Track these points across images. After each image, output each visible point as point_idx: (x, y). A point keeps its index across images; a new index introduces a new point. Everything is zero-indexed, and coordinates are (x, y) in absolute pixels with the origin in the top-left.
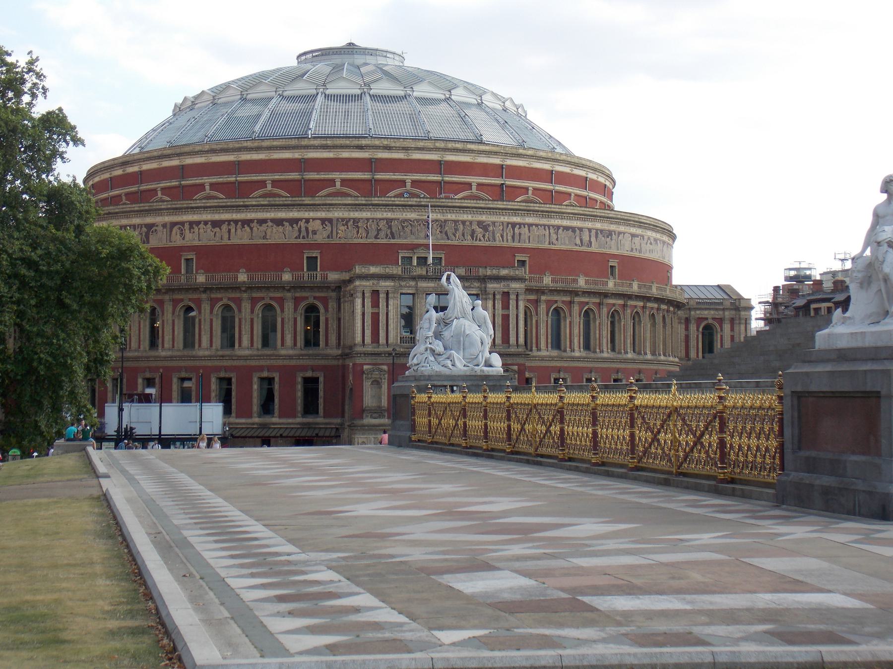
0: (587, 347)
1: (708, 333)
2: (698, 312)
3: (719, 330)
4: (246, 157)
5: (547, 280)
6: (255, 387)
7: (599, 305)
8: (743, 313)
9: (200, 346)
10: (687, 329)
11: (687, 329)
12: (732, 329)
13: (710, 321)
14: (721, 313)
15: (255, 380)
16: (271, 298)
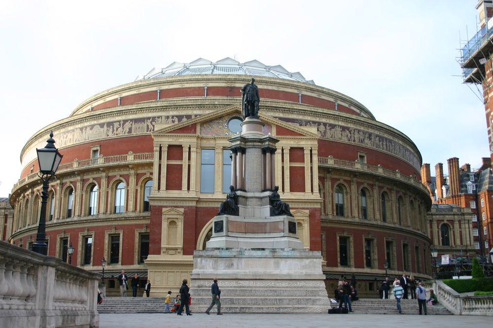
0: (365, 215)
1: (445, 228)
2: (437, 217)
3: (452, 227)
4: (125, 94)
5: (331, 162)
6: (106, 241)
7: (372, 186)
8: (466, 217)
9: (74, 215)
10: (431, 227)
11: (431, 227)
12: (460, 228)
13: (445, 222)
14: (452, 217)
15: (107, 237)
16: (121, 176)
